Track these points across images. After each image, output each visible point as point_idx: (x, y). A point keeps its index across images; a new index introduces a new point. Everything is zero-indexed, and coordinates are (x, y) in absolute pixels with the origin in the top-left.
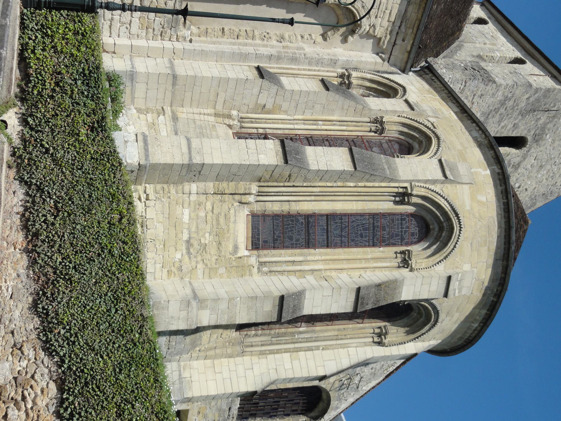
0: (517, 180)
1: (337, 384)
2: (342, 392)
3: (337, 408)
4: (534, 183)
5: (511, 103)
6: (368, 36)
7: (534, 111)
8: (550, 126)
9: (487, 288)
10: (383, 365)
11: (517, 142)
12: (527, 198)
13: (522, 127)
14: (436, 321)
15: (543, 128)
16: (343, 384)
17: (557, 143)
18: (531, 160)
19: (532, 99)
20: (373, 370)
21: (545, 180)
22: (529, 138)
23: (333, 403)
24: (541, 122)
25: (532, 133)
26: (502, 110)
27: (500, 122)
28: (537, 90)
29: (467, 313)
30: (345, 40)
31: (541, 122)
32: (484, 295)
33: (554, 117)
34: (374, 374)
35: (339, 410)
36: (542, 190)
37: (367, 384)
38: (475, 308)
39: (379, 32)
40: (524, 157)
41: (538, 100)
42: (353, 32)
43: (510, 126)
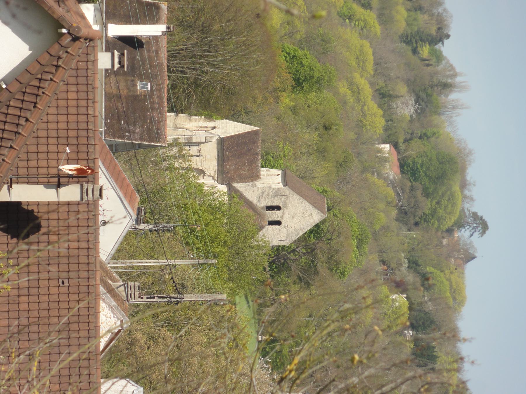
5: (266, 193)
6: (209, 176)
11: (278, 208)
15: (285, 202)
18: (286, 216)
19: (274, 192)
22: (281, 206)
24: (283, 199)
26: (264, 196)
27: (265, 200)
28: (274, 189)
30: (203, 178)
31: (283, 199)
33: (287, 198)
39: (212, 175)
40: (283, 214)
41: (276, 192)
42: (204, 175)
43: (270, 202)
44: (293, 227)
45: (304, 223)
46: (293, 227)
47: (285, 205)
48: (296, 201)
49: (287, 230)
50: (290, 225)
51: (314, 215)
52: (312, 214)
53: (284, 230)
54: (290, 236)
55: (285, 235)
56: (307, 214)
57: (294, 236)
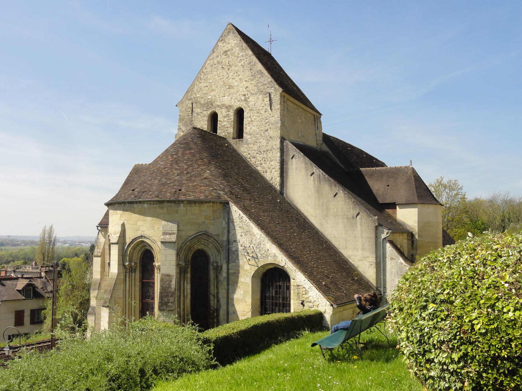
0: (239, 101)
1: (252, 262)
2: (259, 255)
3: (275, 256)
4: (241, 85)
7: (192, 121)
8: (202, 101)
9: (123, 211)
10: (240, 227)
12: (254, 82)
13: (202, 123)
14: (141, 237)
15: (203, 105)
16: (253, 257)
17: (214, 87)
20: (243, 234)
21: (240, 77)
22: (209, 112)
23: (270, 260)
25: (205, 112)
29: (138, 216)
32: (126, 211)
34: (248, 232)
35: (277, 254)
36: (247, 73)
37: (255, 235)
38: (135, 213)
44: (246, 84)
45: (240, 64)
46: (246, 84)
47: (210, 104)
48: (202, 85)
49: (252, 94)
50: (242, 90)
51: (227, 47)
52: (226, 52)
53: (252, 100)
54: (262, 87)
55: (261, 96)
56: (225, 60)
57: (262, 80)
